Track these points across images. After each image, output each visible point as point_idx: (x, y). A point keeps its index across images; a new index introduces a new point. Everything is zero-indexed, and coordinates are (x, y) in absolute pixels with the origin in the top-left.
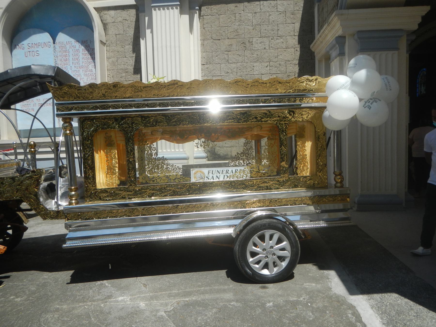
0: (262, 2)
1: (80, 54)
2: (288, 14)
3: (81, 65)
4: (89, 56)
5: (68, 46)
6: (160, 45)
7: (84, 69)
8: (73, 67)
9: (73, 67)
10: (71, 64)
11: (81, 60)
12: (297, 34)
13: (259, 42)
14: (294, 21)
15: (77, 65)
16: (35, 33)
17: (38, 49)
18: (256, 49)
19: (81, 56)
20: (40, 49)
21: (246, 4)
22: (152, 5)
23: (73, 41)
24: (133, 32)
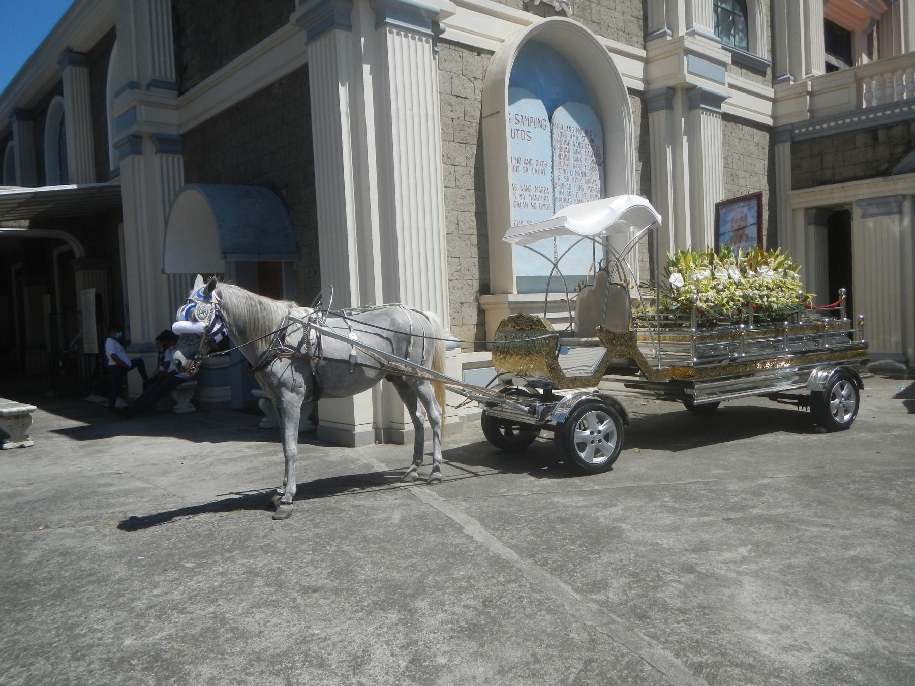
0: (744, 126)
1: (583, 151)
2: (760, 148)
3: (583, 170)
4: (594, 158)
5: (569, 134)
6: (707, 165)
7: (587, 178)
8: (574, 171)
9: (574, 171)
10: (572, 168)
11: (583, 163)
12: (766, 174)
13: (742, 176)
14: (764, 157)
15: (578, 170)
16: (526, 97)
17: (529, 129)
18: (741, 185)
19: (583, 157)
20: (531, 129)
21: (733, 124)
22: (702, 106)
23: (575, 125)
24: (639, 133)
